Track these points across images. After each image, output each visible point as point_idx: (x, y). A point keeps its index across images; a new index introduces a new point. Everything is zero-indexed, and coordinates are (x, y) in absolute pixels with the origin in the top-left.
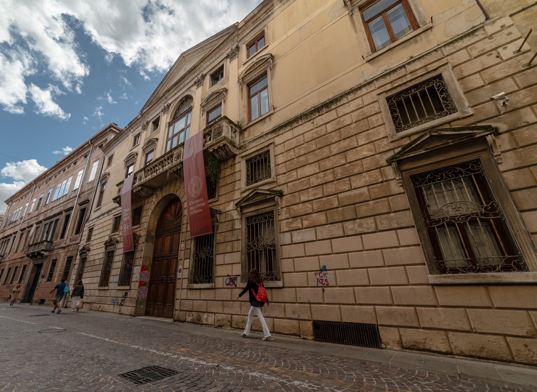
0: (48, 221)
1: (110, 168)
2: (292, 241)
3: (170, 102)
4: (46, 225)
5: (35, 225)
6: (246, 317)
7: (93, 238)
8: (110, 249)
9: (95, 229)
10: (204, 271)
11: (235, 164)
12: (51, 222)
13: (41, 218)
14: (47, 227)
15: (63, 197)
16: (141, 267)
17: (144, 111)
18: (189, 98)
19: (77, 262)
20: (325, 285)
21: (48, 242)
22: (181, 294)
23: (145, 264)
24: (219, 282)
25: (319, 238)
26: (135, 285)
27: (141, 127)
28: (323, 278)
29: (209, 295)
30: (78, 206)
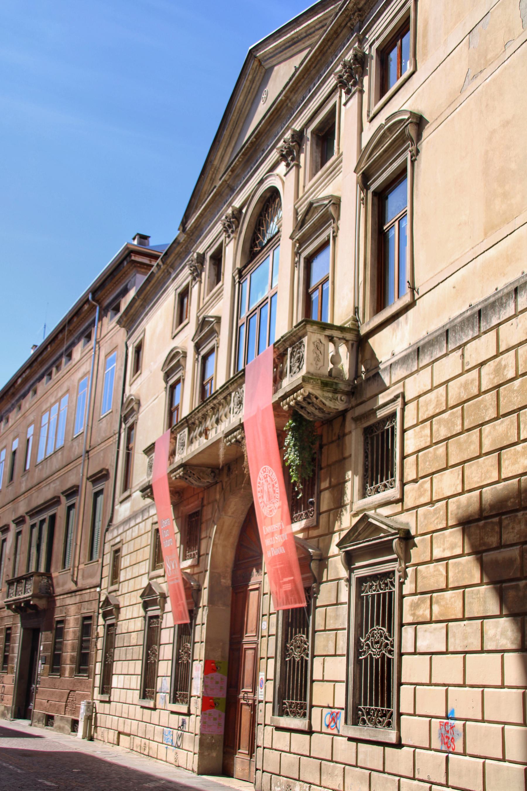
0: (37, 520)
1: (139, 381)
2: (447, 649)
3: (237, 204)
4: (33, 526)
5: (13, 526)
6: (63, 713)
7: (122, 576)
8: (153, 611)
9: (124, 551)
10: (294, 691)
11: (344, 435)
12: (42, 522)
13: (22, 509)
14: (35, 531)
15: (55, 452)
16: (202, 663)
17: (192, 221)
18: (272, 197)
19: (101, 631)
20: (451, 750)
21: (42, 575)
22: (265, 736)
23: (212, 658)
24: (413, 729)
25: (451, 649)
26: (196, 705)
27: (187, 271)
28: (449, 735)
29: (300, 742)
30: (89, 484)
